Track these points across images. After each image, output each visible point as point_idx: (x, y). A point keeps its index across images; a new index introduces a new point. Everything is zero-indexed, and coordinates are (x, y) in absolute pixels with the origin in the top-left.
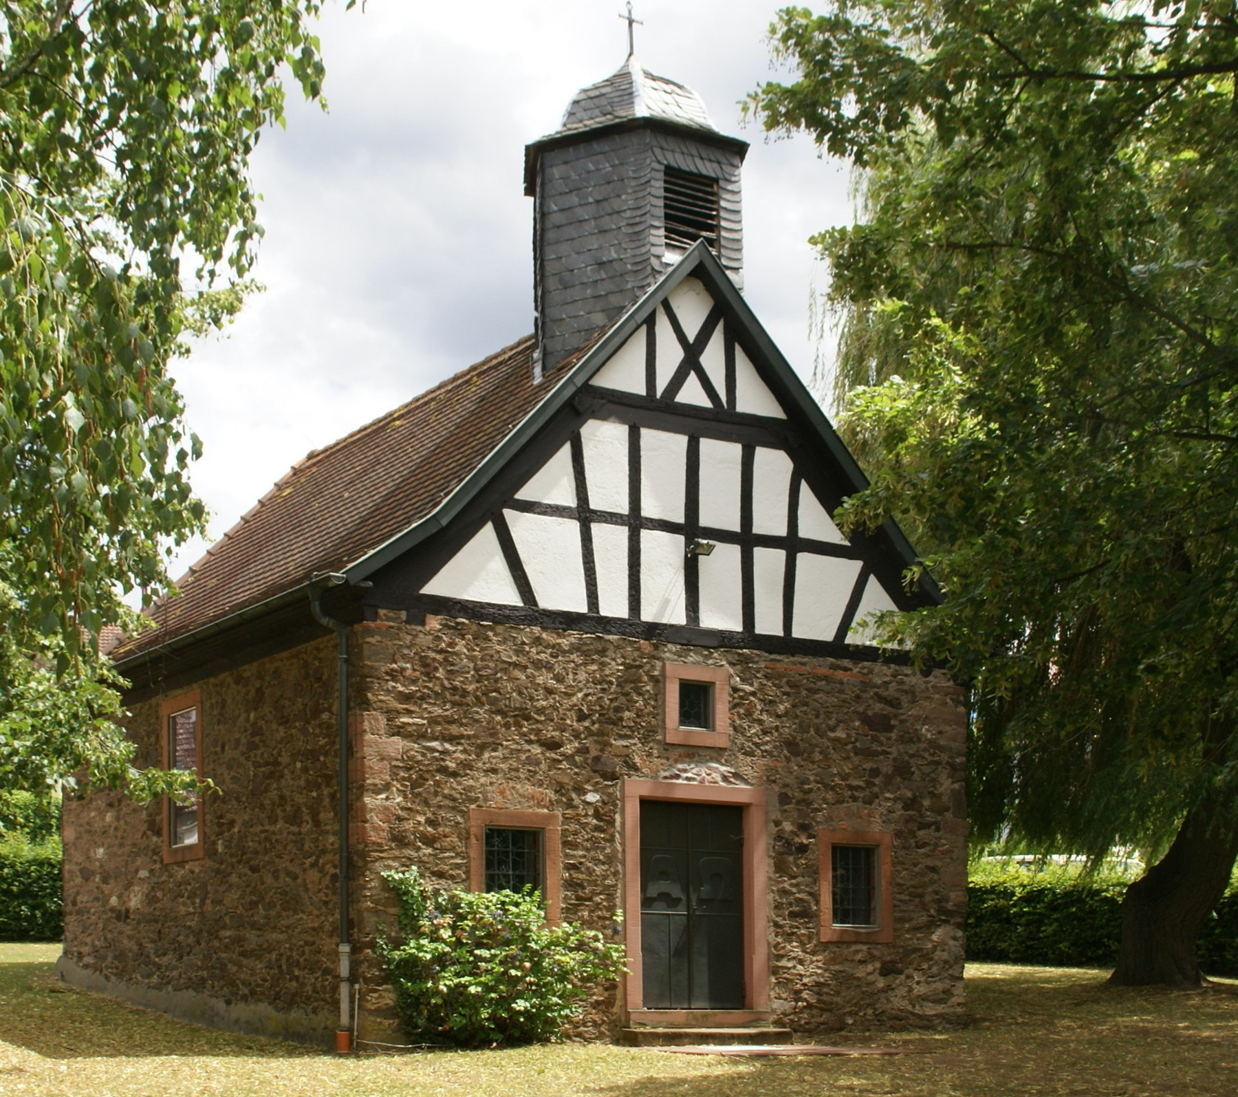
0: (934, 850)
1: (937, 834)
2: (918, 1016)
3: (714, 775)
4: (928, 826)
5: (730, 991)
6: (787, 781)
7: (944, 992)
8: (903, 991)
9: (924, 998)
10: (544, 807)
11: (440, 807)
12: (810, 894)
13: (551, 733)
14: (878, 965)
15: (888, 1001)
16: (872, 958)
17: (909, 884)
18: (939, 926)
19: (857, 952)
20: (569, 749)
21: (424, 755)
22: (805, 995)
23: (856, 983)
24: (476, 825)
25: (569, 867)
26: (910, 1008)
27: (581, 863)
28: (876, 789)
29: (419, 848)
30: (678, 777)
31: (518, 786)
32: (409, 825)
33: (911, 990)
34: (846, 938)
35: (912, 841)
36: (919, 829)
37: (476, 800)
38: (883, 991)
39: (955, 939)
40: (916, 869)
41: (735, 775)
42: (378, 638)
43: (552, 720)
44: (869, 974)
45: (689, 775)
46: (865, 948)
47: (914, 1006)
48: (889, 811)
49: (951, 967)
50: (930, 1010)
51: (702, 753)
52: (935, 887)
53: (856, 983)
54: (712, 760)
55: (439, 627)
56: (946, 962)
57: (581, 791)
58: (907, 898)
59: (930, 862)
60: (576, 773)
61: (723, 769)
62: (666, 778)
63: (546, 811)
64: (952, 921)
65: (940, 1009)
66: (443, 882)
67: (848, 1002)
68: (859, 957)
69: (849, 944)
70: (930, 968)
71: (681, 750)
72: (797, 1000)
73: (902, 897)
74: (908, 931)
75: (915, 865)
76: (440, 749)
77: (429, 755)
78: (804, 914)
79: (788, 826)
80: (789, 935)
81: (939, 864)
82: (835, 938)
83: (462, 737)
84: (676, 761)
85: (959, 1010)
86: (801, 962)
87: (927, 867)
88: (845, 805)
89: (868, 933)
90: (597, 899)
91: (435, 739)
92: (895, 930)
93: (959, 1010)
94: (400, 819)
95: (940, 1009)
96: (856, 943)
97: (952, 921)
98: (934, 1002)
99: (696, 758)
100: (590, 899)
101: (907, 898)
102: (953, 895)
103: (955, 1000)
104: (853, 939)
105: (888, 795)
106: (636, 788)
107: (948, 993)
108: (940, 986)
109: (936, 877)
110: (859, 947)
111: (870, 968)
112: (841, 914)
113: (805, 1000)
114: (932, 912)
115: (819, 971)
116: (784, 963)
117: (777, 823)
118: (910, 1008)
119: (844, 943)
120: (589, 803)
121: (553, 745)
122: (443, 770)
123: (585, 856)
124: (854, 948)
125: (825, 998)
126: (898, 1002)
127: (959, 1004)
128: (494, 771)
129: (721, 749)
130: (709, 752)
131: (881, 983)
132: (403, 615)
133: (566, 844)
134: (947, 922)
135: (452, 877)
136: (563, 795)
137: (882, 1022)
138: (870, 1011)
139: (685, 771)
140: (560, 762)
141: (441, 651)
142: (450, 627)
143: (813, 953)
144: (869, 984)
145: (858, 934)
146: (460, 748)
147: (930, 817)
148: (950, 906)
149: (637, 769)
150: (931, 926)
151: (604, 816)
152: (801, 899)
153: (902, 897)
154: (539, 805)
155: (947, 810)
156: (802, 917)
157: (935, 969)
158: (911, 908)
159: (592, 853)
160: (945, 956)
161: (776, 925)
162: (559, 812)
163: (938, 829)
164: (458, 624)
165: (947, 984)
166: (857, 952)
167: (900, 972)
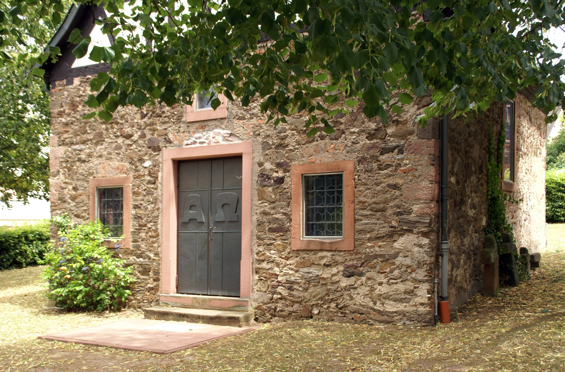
0: (396, 170)
1: (400, 156)
2: (379, 312)
3: (217, 137)
4: (392, 150)
5: (230, 284)
6: (269, 133)
7: (405, 292)
8: (364, 290)
9: (387, 297)
10: (124, 173)
11: (78, 180)
12: (284, 214)
13: (128, 130)
14: (341, 268)
15: (352, 298)
16: (336, 264)
17: (370, 201)
18: (401, 235)
19: (322, 258)
20: (136, 137)
21: (72, 153)
22: (280, 289)
23: (322, 282)
24: (91, 187)
25: (136, 207)
26: (371, 304)
27: (141, 204)
28: (342, 127)
29: (69, 203)
30: (195, 142)
31: (111, 163)
32: (66, 191)
33: (372, 289)
34: (312, 247)
35: (375, 165)
36: (382, 154)
37: (93, 174)
38: (345, 289)
39: (421, 246)
40: (378, 188)
41: (231, 135)
42: (55, 97)
43: (127, 122)
44: (333, 275)
45: (201, 140)
46: (329, 254)
47: (375, 303)
48: (353, 143)
49: (413, 271)
50: (391, 307)
51: (210, 123)
52: (396, 202)
53: (322, 282)
54: (216, 127)
55: (79, 83)
56: (408, 267)
57: (141, 160)
58: (369, 213)
59: (391, 181)
60: (139, 151)
61: (222, 132)
62: (187, 145)
63: (125, 175)
64: (415, 231)
65: (401, 307)
66: (79, 220)
67: (314, 297)
68: (323, 262)
69: (315, 251)
70: (392, 271)
71: (197, 125)
72: (274, 293)
73: (365, 212)
74: (369, 240)
75: (377, 185)
76: (79, 149)
77: (74, 153)
78: (281, 230)
79: (268, 166)
80: (268, 245)
81: (400, 181)
82: (303, 247)
83: (88, 140)
84: (194, 133)
85: (421, 309)
86: (278, 265)
87: (389, 185)
88: (315, 143)
89: (331, 243)
90: (149, 225)
91: (77, 144)
92: (355, 240)
93: (421, 309)
94: (63, 188)
95: (401, 307)
96: (322, 250)
97: (415, 231)
98: (395, 300)
99: (207, 129)
100: (145, 226)
101: (369, 213)
102: (415, 208)
103: (418, 300)
104: (318, 248)
105: (352, 130)
106: (168, 155)
107: (411, 292)
108: (401, 287)
109: (398, 193)
110: (325, 253)
111: (335, 270)
112: (311, 229)
113: (280, 294)
114: (394, 223)
115: (291, 272)
116: (264, 265)
117: (261, 164)
118: (371, 304)
119: (311, 250)
120: (146, 168)
121: (129, 136)
122: (79, 160)
123: (143, 200)
124: (320, 254)
125: (294, 293)
126: (360, 298)
127: (422, 304)
128: (101, 156)
129: (222, 119)
130: (214, 123)
131: (345, 282)
132: (65, 82)
133: (135, 193)
134: (410, 231)
135: (83, 217)
136: (133, 164)
137: (345, 315)
138: (333, 305)
139: (200, 138)
140: (131, 145)
141: (80, 96)
142: (84, 82)
143: (287, 258)
144: (333, 283)
145: (322, 243)
146: (88, 146)
147: (393, 142)
148: (412, 217)
149: (170, 142)
150: (392, 235)
151: (153, 175)
152: (277, 219)
153: (365, 212)
154: (121, 172)
155: (411, 133)
156: (278, 232)
157: (396, 273)
158: (373, 221)
159: (147, 197)
160: (408, 261)
161: (259, 238)
162: (131, 174)
163: (401, 152)
164: (88, 79)
165: (409, 285)
166: (322, 258)
167: (361, 274)
